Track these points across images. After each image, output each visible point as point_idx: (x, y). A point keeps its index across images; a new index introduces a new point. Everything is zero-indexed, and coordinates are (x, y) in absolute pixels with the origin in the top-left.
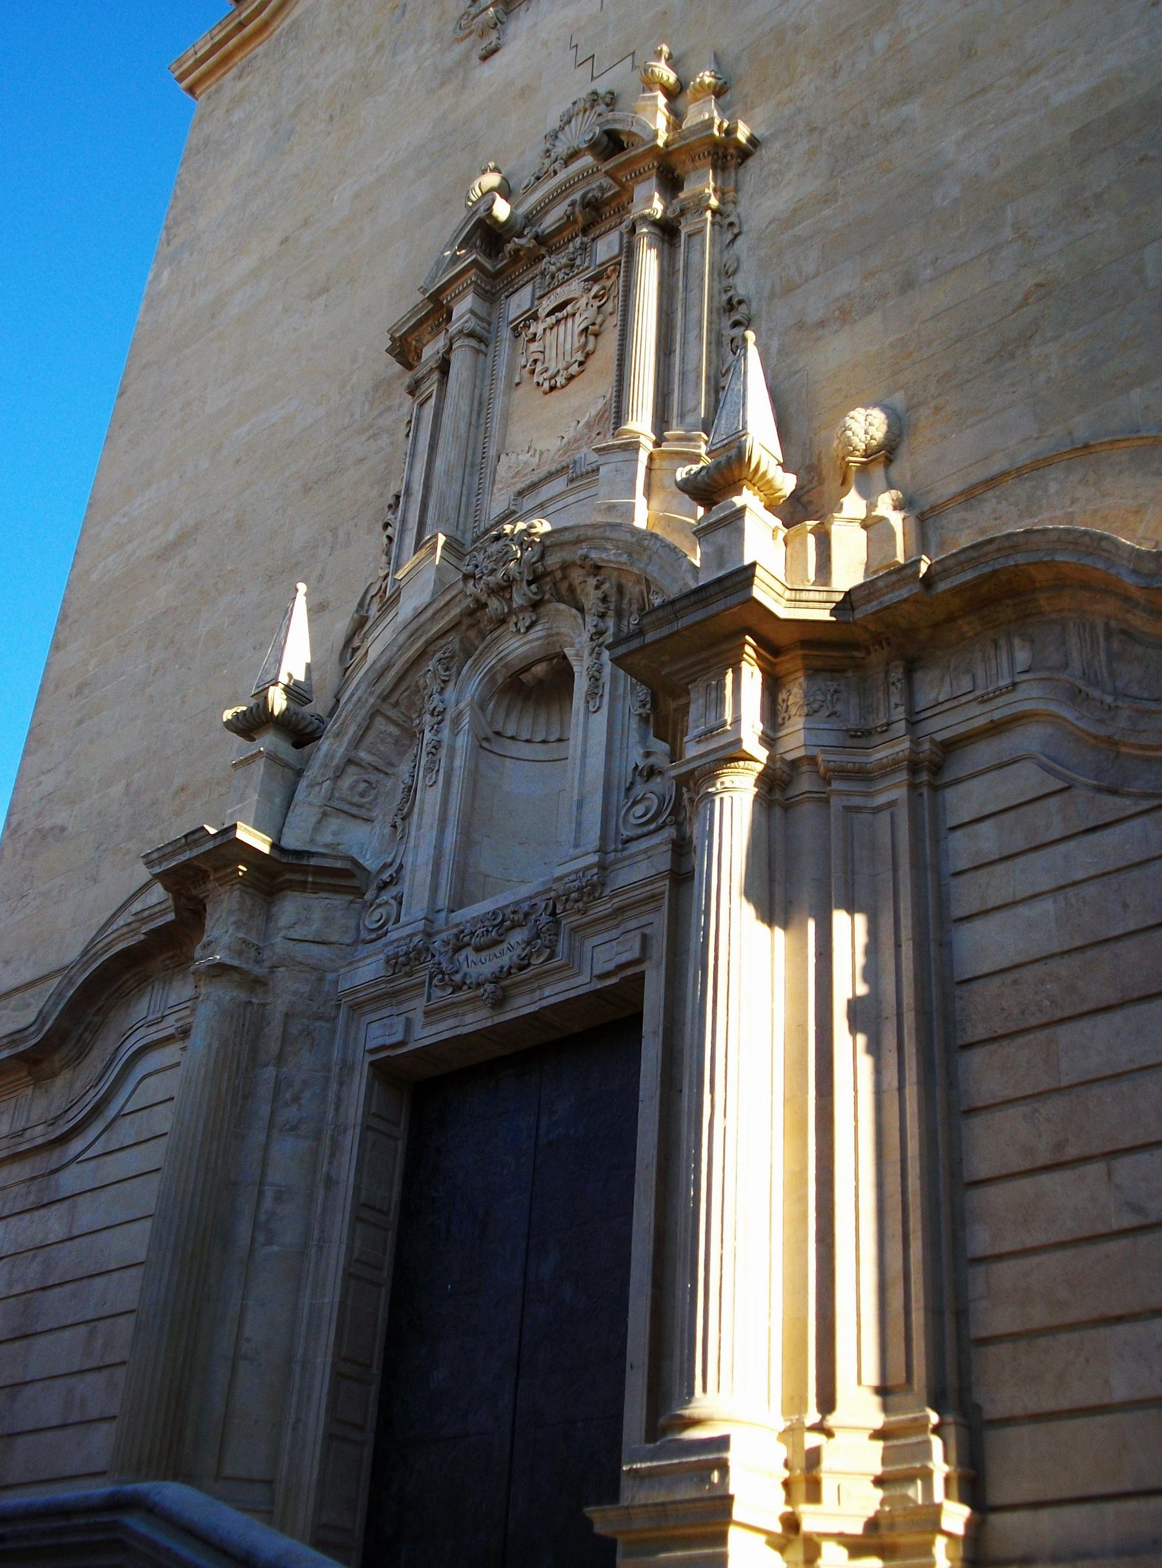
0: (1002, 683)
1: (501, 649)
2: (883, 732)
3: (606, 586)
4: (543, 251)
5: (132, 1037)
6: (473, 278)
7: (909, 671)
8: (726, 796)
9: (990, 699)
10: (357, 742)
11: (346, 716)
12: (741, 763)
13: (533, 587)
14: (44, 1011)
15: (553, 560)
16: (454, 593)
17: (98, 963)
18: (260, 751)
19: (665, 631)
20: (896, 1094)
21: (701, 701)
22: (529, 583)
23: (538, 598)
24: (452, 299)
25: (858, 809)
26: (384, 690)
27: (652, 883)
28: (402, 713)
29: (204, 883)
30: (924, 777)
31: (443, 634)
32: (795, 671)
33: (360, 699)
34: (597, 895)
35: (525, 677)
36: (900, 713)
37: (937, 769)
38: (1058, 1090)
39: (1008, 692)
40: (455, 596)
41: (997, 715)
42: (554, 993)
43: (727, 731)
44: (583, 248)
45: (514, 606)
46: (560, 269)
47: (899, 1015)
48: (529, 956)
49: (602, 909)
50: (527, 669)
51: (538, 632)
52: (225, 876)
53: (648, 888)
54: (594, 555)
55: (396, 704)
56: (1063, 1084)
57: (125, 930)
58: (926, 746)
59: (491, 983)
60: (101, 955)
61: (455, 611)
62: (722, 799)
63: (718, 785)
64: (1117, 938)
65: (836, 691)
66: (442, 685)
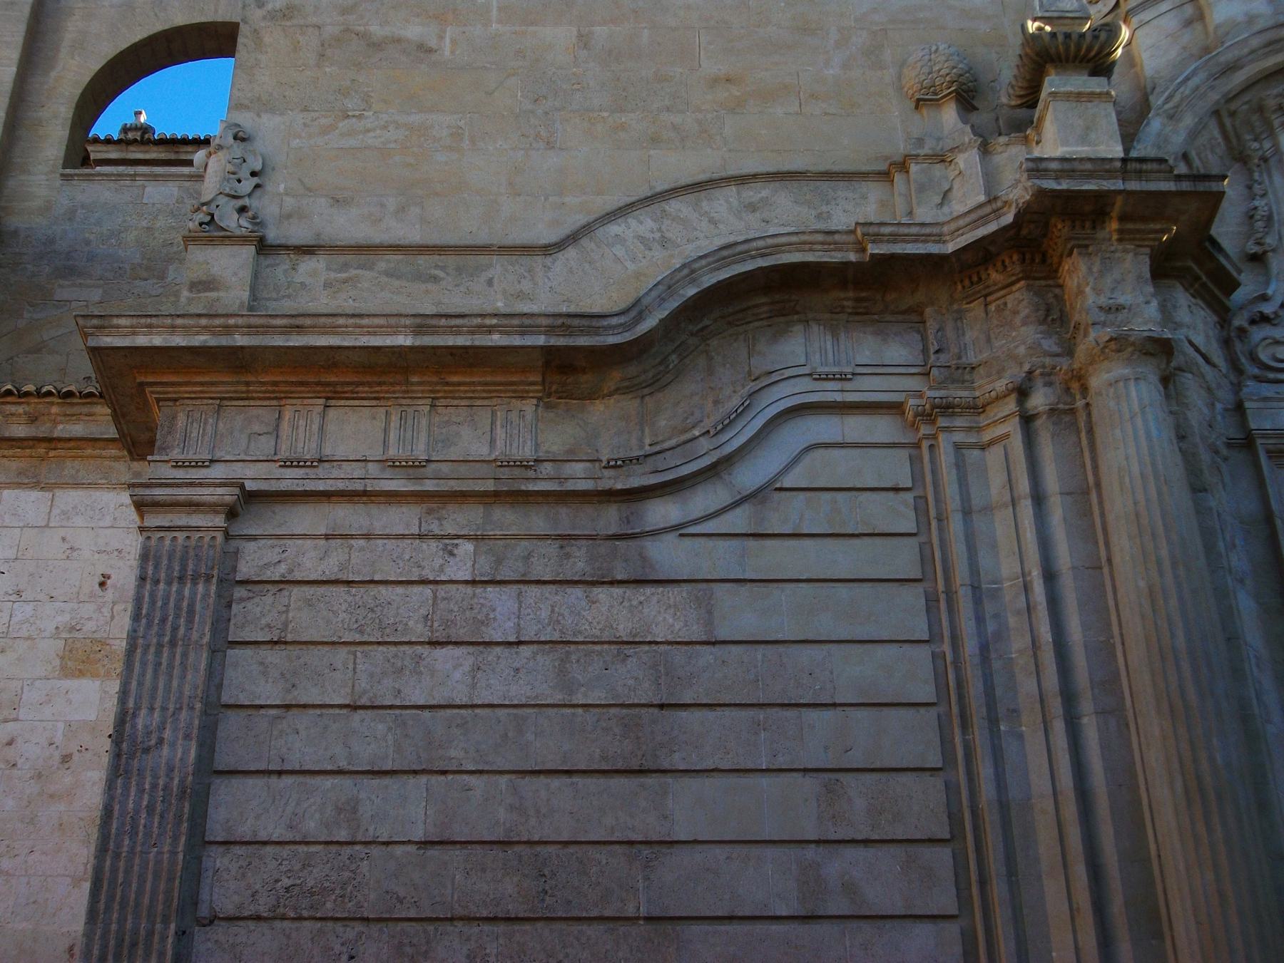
5: (775, 388)
10: (1193, 134)
11: (1182, 100)
14: (646, 301)
17: (749, 266)
18: (1108, 93)
26: (1229, 92)
28: (1233, 126)
29: (1094, 228)
33: (1197, 88)
52: (1138, 231)
55: (1233, 114)
57: (820, 238)
60: (753, 257)
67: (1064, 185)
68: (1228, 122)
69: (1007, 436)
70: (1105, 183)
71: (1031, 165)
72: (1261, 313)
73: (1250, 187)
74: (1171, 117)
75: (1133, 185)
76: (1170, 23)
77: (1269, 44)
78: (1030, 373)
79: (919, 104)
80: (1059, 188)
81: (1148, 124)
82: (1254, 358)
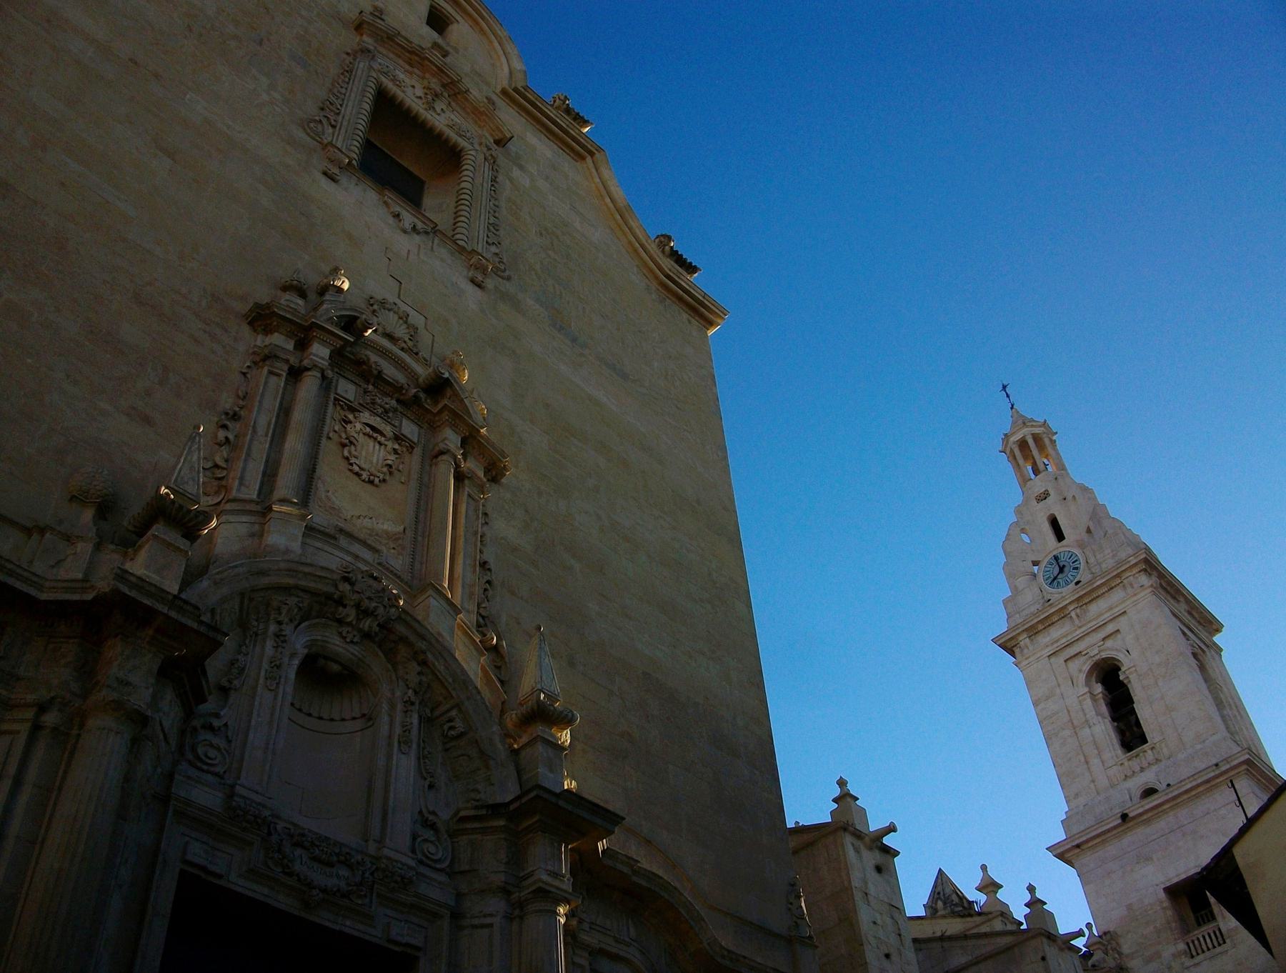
3: (424, 679)
4: (372, 380)
6: (338, 346)
15: (401, 629)
16: (329, 576)
18: (187, 552)
19: (569, 807)
22: (379, 625)
24: (319, 338)
31: (305, 590)
35: (322, 662)
40: (325, 578)
41: (621, 953)
42: (350, 926)
43: (564, 881)
44: (395, 410)
46: (381, 406)
50: (326, 658)
51: (354, 649)
55: (251, 600)
67: (133, 594)
68: (246, 602)
69: (18, 732)
70: (157, 604)
71: (119, 571)
72: (211, 724)
73: (240, 646)
74: (215, 583)
75: (173, 614)
76: (243, 530)
77: (289, 570)
78: (53, 698)
79: (73, 498)
80: (129, 594)
81: (201, 581)
82: (194, 749)
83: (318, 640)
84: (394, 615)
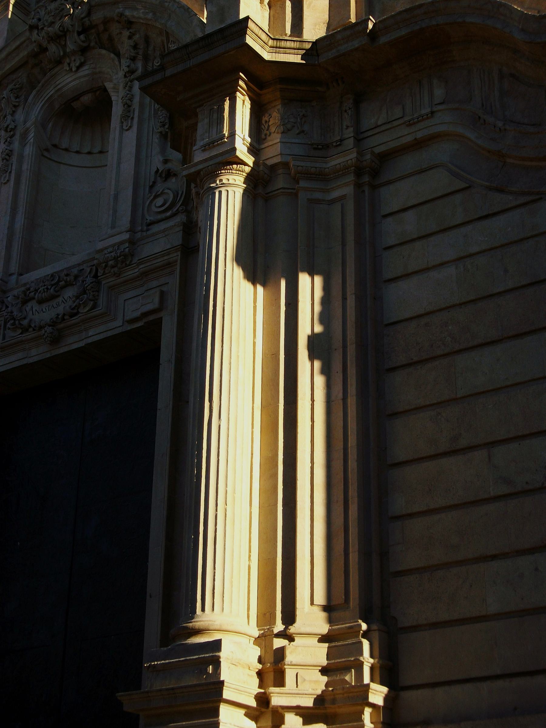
0: (423, 112)
1: (57, 83)
2: (337, 146)
7: (357, 102)
8: (223, 190)
9: (414, 123)
12: (235, 166)
13: (82, 37)
15: (97, 16)
16: (22, 39)
20: (341, 402)
21: (206, 121)
22: (79, 34)
23: (85, 45)
25: (318, 201)
27: (169, 254)
30: (366, 179)
32: (275, 100)
34: (128, 263)
35: (76, 105)
36: (349, 133)
37: (375, 173)
38: (455, 399)
39: (428, 118)
40: (24, 41)
41: (419, 135)
45: (68, 50)
47: (345, 347)
48: (78, 306)
49: (131, 273)
50: (77, 98)
51: (85, 71)
53: (166, 258)
54: (128, 13)
56: (459, 396)
58: (368, 157)
59: (50, 326)
61: (24, 53)
62: (220, 192)
63: (218, 182)
64: (499, 294)
65: (304, 115)
66: (14, 109)
83: (51, 96)
84: (82, 14)
